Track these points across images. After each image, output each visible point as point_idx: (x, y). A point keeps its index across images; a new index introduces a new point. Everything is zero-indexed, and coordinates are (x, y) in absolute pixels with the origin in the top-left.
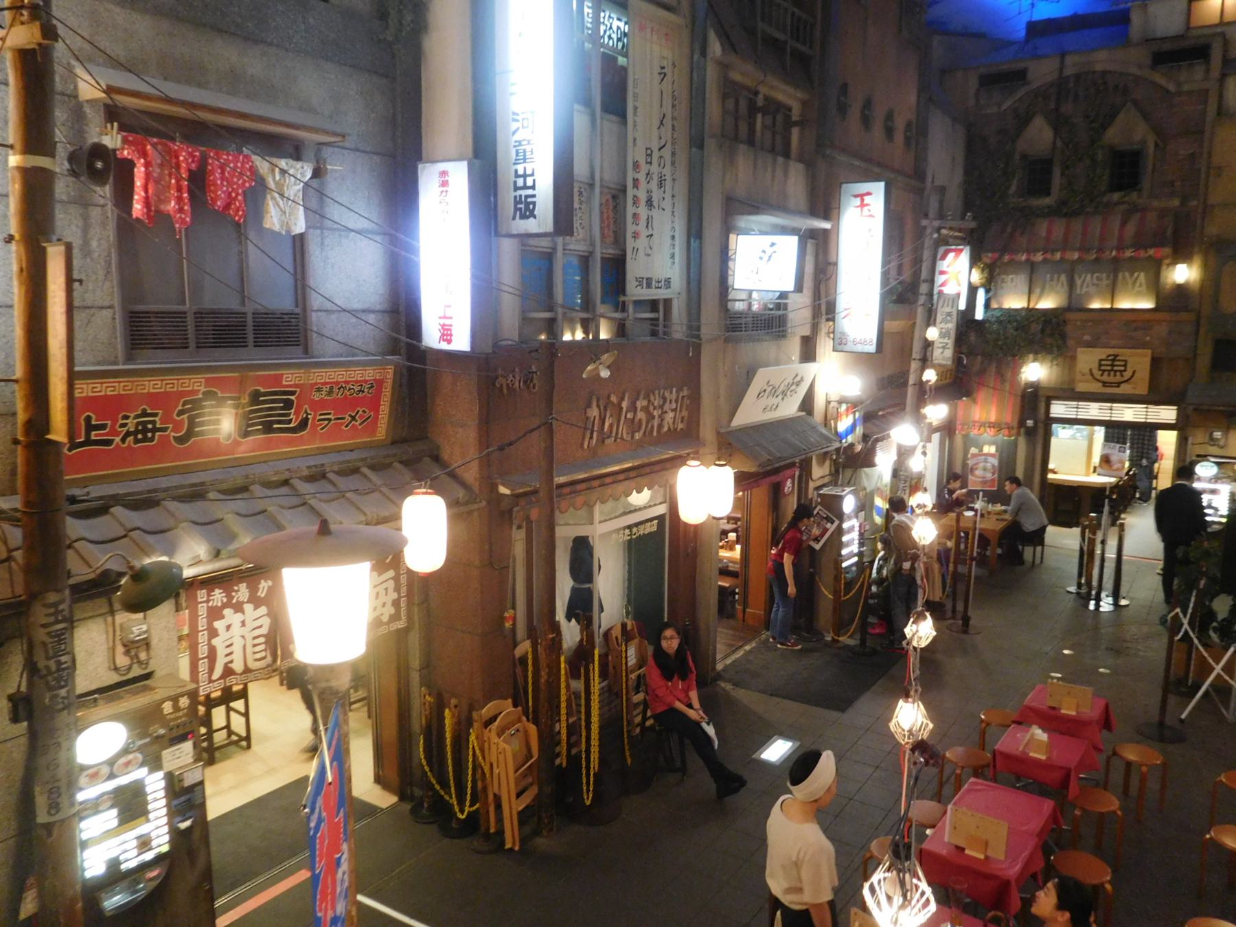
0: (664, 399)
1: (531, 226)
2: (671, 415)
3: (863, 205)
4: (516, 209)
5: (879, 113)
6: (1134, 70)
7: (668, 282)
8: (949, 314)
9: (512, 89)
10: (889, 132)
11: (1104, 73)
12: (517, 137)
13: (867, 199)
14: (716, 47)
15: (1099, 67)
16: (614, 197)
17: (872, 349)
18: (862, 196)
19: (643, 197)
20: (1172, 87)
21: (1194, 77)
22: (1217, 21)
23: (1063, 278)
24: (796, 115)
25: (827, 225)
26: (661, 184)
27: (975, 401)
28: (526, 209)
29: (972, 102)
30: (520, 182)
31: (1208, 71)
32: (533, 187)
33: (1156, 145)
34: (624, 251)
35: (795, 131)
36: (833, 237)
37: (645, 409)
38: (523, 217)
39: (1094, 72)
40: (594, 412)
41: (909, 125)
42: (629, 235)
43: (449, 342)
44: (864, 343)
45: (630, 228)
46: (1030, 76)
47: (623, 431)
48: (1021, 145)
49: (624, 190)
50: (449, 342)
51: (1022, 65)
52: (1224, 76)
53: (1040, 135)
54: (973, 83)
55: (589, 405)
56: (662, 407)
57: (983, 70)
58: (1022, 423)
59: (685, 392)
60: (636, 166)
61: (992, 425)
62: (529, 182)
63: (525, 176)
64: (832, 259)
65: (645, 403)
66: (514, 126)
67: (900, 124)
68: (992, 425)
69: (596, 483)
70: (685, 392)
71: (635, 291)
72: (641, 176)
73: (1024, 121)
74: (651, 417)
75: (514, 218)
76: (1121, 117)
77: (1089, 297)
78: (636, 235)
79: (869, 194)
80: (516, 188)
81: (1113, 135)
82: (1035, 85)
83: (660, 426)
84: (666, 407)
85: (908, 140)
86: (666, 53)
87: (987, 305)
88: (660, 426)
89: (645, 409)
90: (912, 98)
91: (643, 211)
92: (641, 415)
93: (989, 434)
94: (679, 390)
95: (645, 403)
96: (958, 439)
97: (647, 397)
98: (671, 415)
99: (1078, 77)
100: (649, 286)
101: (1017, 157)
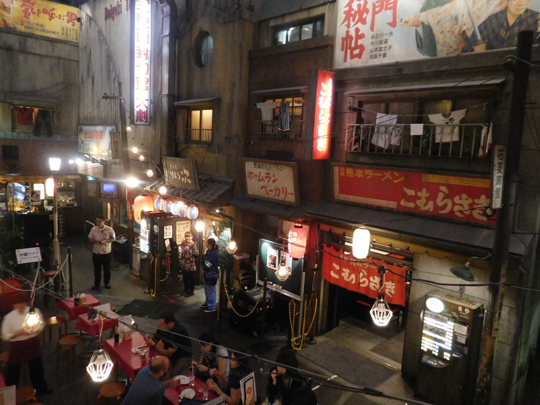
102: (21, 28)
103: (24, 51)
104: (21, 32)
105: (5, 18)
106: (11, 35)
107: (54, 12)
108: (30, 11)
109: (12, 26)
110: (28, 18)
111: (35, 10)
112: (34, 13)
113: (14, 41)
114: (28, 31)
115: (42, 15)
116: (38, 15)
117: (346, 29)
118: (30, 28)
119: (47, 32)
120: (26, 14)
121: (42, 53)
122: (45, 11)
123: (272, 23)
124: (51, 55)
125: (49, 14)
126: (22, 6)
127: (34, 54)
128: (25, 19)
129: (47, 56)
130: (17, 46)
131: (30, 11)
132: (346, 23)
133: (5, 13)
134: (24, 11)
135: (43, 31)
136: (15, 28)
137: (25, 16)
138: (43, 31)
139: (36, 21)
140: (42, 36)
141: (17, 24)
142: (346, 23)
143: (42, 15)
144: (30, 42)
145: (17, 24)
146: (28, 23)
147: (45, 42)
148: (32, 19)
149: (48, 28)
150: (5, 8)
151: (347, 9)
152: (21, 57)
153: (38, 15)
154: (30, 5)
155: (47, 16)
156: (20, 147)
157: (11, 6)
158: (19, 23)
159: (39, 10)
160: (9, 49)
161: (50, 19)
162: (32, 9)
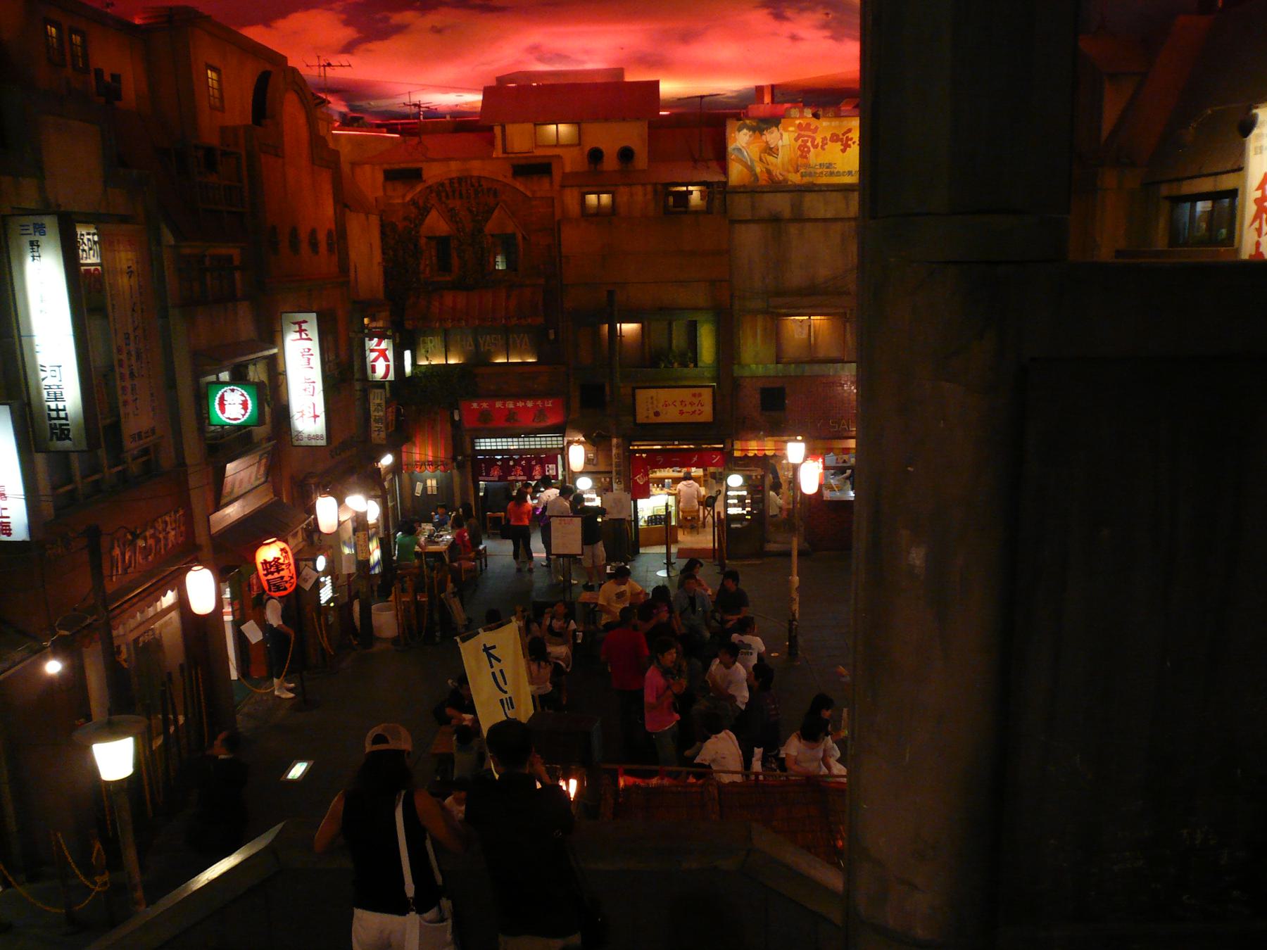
0: (166, 523)
1: (67, 444)
2: (173, 533)
3: (301, 331)
4: (53, 433)
5: (304, 235)
6: (501, 178)
7: (153, 431)
8: (379, 405)
9: (37, 349)
10: (314, 245)
11: (479, 178)
12: (45, 383)
13: (304, 326)
14: (168, 238)
15: (475, 173)
16: (105, 376)
17: (323, 443)
18: (299, 323)
19: (126, 371)
20: (529, 194)
21: (541, 187)
22: (554, 142)
23: (470, 339)
24: (236, 263)
25: (275, 351)
26: (138, 357)
27: (414, 444)
28: (62, 432)
29: (380, 193)
30: (54, 414)
31: (551, 183)
32: (66, 418)
33: (524, 237)
34: (118, 416)
35: (237, 275)
36: (280, 358)
37: (153, 536)
38: (59, 439)
39: (472, 177)
40: (117, 551)
41: (330, 234)
42: (121, 404)
43: (9, 535)
44: (316, 437)
45: (121, 399)
46: (425, 176)
47: (139, 558)
48: (424, 230)
49: (112, 368)
50: (9, 535)
51: (419, 165)
52: (563, 187)
53: (436, 223)
54: (380, 177)
55: (112, 548)
56: (164, 530)
57: (386, 166)
58: (454, 459)
59: (181, 512)
60: (120, 351)
61: (431, 463)
62: (62, 414)
63: (58, 410)
64: (281, 369)
65: (152, 531)
66: (42, 375)
67: (322, 237)
68: (431, 463)
69: (126, 606)
70: (181, 512)
71: (130, 446)
72: (124, 357)
73: (424, 211)
74: (158, 541)
75: (51, 439)
76: (496, 213)
77: (490, 354)
78: (125, 403)
79: (305, 322)
80: (51, 418)
81: (490, 227)
82: (430, 182)
83: (166, 545)
84: (169, 528)
85: (330, 248)
86: (130, 255)
87: (414, 363)
88: (166, 545)
89: (153, 536)
90: (329, 210)
91: (128, 383)
92: (151, 542)
93: (428, 472)
94: (177, 512)
95: (152, 531)
96: (405, 475)
97: (153, 527)
98: (173, 533)
99: (460, 179)
100: (140, 438)
101: (423, 241)
102: (795, 178)
103: (799, 218)
104: (795, 185)
105: (771, 168)
106: (779, 195)
107: (850, 135)
108: (809, 144)
109: (781, 178)
110: (806, 157)
111: (819, 140)
112: (816, 147)
113: (782, 204)
114: (807, 180)
115: (830, 145)
116: (823, 149)
117: (1256, 238)
118: (810, 175)
119: (838, 174)
120: (802, 151)
121: (829, 216)
122: (835, 138)
123: (1165, 190)
124: (846, 216)
125: (841, 140)
126: (796, 139)
127: (816, 220)
128: (800, 161)
129: (835, 220)
130: (787, 214)
131: (809, 144)
132: (1257, 224)
133: (770, 159)
134: (799, 148)
135: (832, 174)
136: (786, 180)
137: (801, 156)
138: (832, 174)
139: (820, 160)
140: (827, 185)
141: (789, 172)
142: (1257, 224)
143: (830, 145)
144: (809, 199)
145: (789, 172)
146: (807, 166)
147: (835, 194)
148: (814, 157)
149: (839, 167)
150: (771, 149)
151: (1258, 194)
152: (793, 229)
153: (823, 149)
154: (810, 133)
155: (839, 146)
156: (787, 391)
157: (780, 143)
158: (791, 169)
159: (824, 139)
160: (775, 220)
161: (844, 151)
162: (813, 140)
